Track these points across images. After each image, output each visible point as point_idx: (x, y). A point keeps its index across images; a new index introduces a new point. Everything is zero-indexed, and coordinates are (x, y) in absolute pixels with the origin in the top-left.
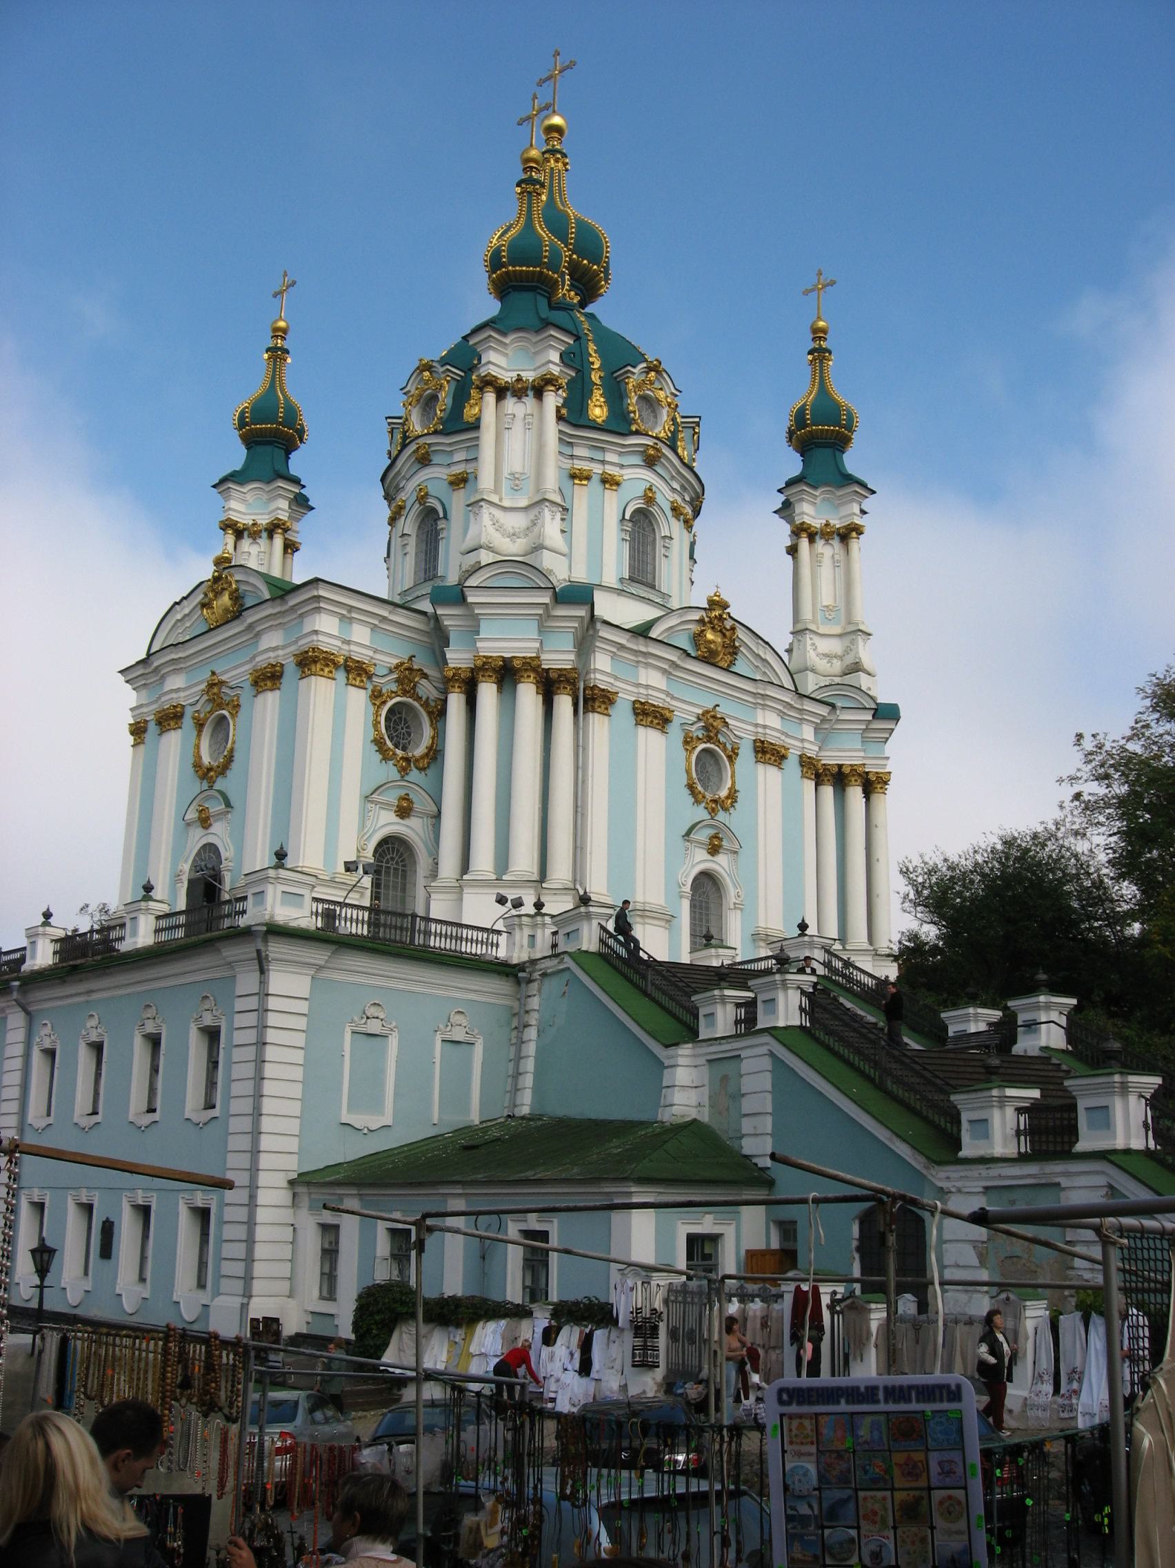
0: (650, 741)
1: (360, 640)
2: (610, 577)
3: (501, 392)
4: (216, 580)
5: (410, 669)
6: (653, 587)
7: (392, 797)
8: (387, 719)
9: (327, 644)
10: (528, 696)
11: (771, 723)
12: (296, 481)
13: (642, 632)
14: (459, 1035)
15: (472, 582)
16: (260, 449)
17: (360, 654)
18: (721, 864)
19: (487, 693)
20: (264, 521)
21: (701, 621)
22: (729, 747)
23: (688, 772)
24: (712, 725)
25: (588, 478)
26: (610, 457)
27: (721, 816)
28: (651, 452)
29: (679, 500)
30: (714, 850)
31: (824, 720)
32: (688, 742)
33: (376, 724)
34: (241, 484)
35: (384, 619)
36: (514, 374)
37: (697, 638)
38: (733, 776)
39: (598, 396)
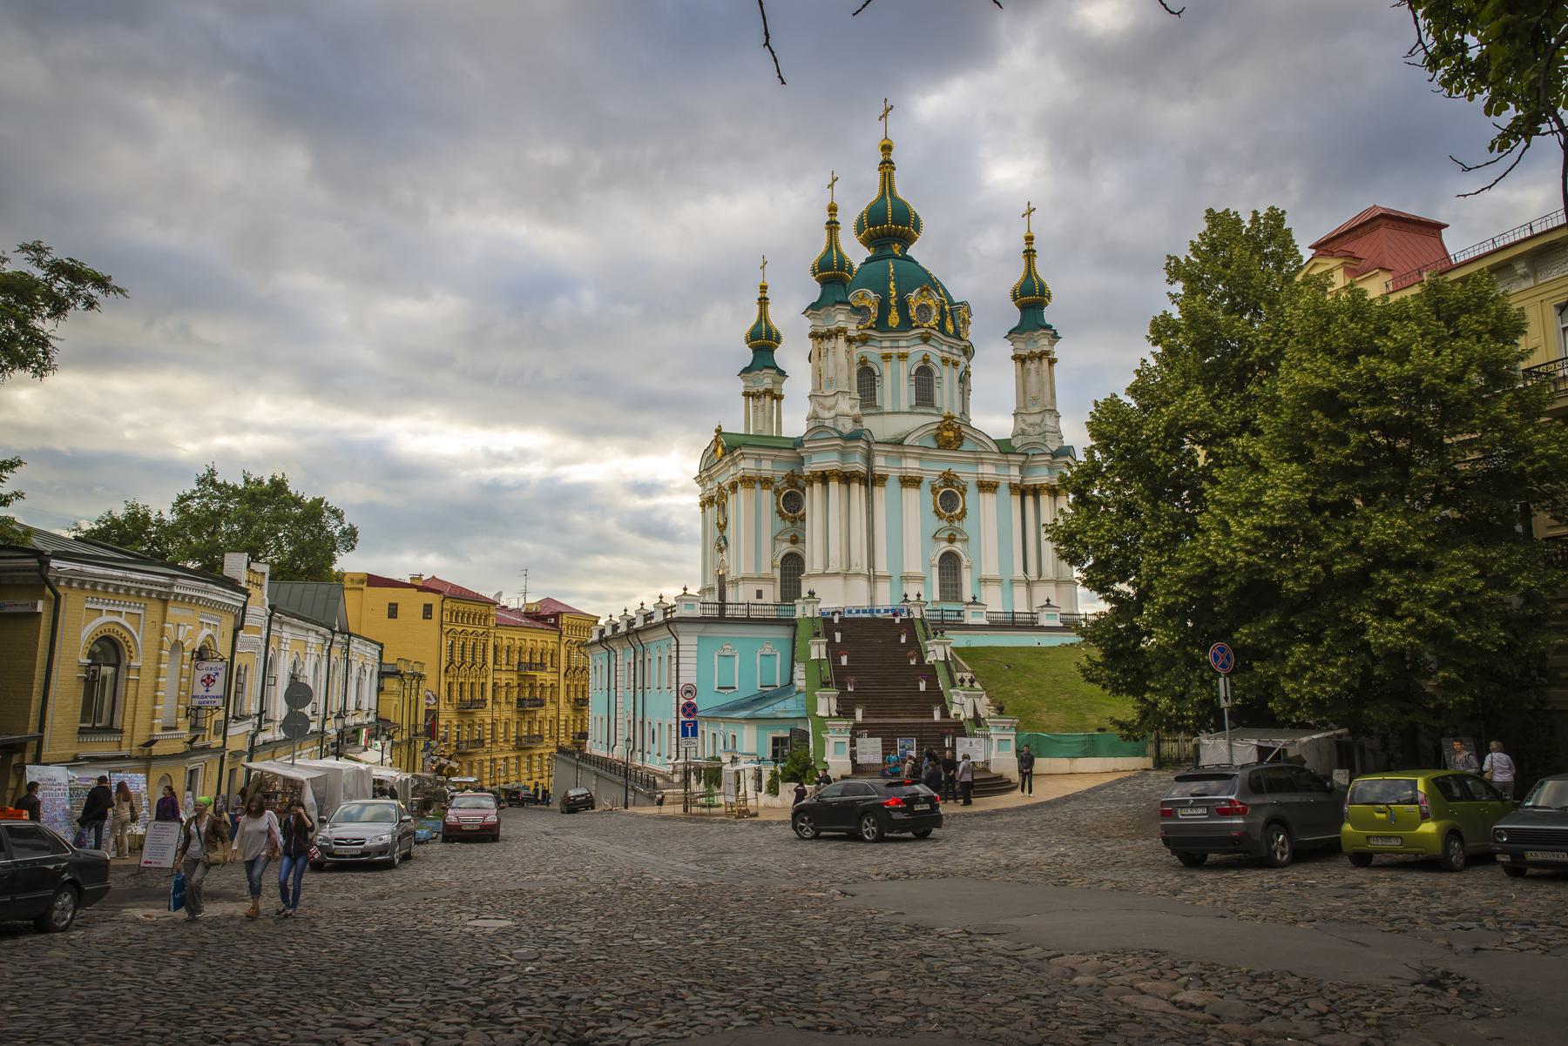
0: (911, 496)
1: (767, 468)
2: (905, 407)
6: (932, 406)
7: (788, 537)
10: (834, 486)
11: (988, 471)
12: (775, 367)
13: (899, 443)
14: (767, 652)
17: (768, 474)
18: (957, 547)
19: (817, 486)
24: (948, 479)
26: (902, 343)
27: (956, 524)
30: (951, 540)
32: (934, 490)
37: (936, 437)
39: (894, 313)
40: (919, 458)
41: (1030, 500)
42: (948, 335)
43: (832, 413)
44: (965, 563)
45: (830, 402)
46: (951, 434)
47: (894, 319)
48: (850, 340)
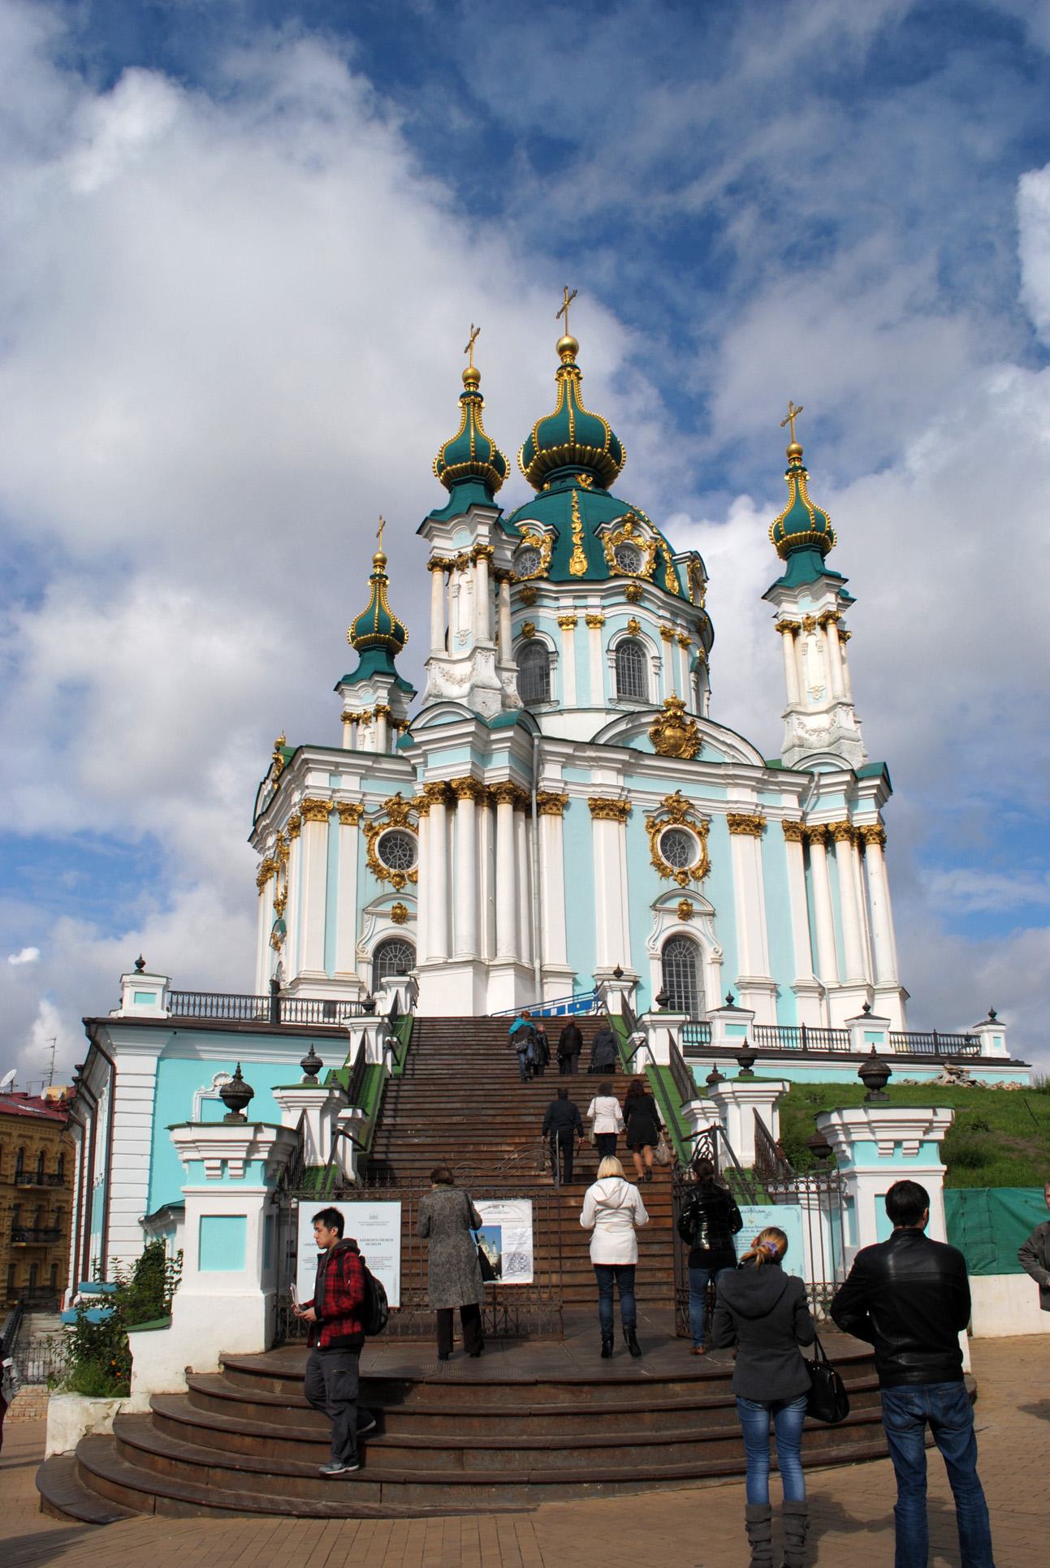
0: (606, 831)
3: (448, 568)
4: (277, 760)
5: (399, 804)
6: (647, 703)
7: (387, 908)
8: (381, 845)
9: (316, 795)
12: (395, 675)
15: (417, 725)
16: (366, 654)
17: (353, 799)
18: (696, 927)
20: (371, 709)
21: (657, 722)
22: (699, 825)
23: (653, 849)
24: (677, 808)
25: (575, 623)
27: (693, 885)
28: (632, 589)
29: (669, 625)
30: (686, 914)
31: (806, 788)
33: (369, 851)
34: (352, 684)
35: (368, 768)
36: (456, 553)
38: (704, 849)
39: (578, 553)
40: (625, 770)
41: (817, 850)
42: (668, 593)
43: (466, 687)
44: (708, 955)
45: (463, 669)
46: (678, 733)
47: (578, 565)
48: (497, 576)
